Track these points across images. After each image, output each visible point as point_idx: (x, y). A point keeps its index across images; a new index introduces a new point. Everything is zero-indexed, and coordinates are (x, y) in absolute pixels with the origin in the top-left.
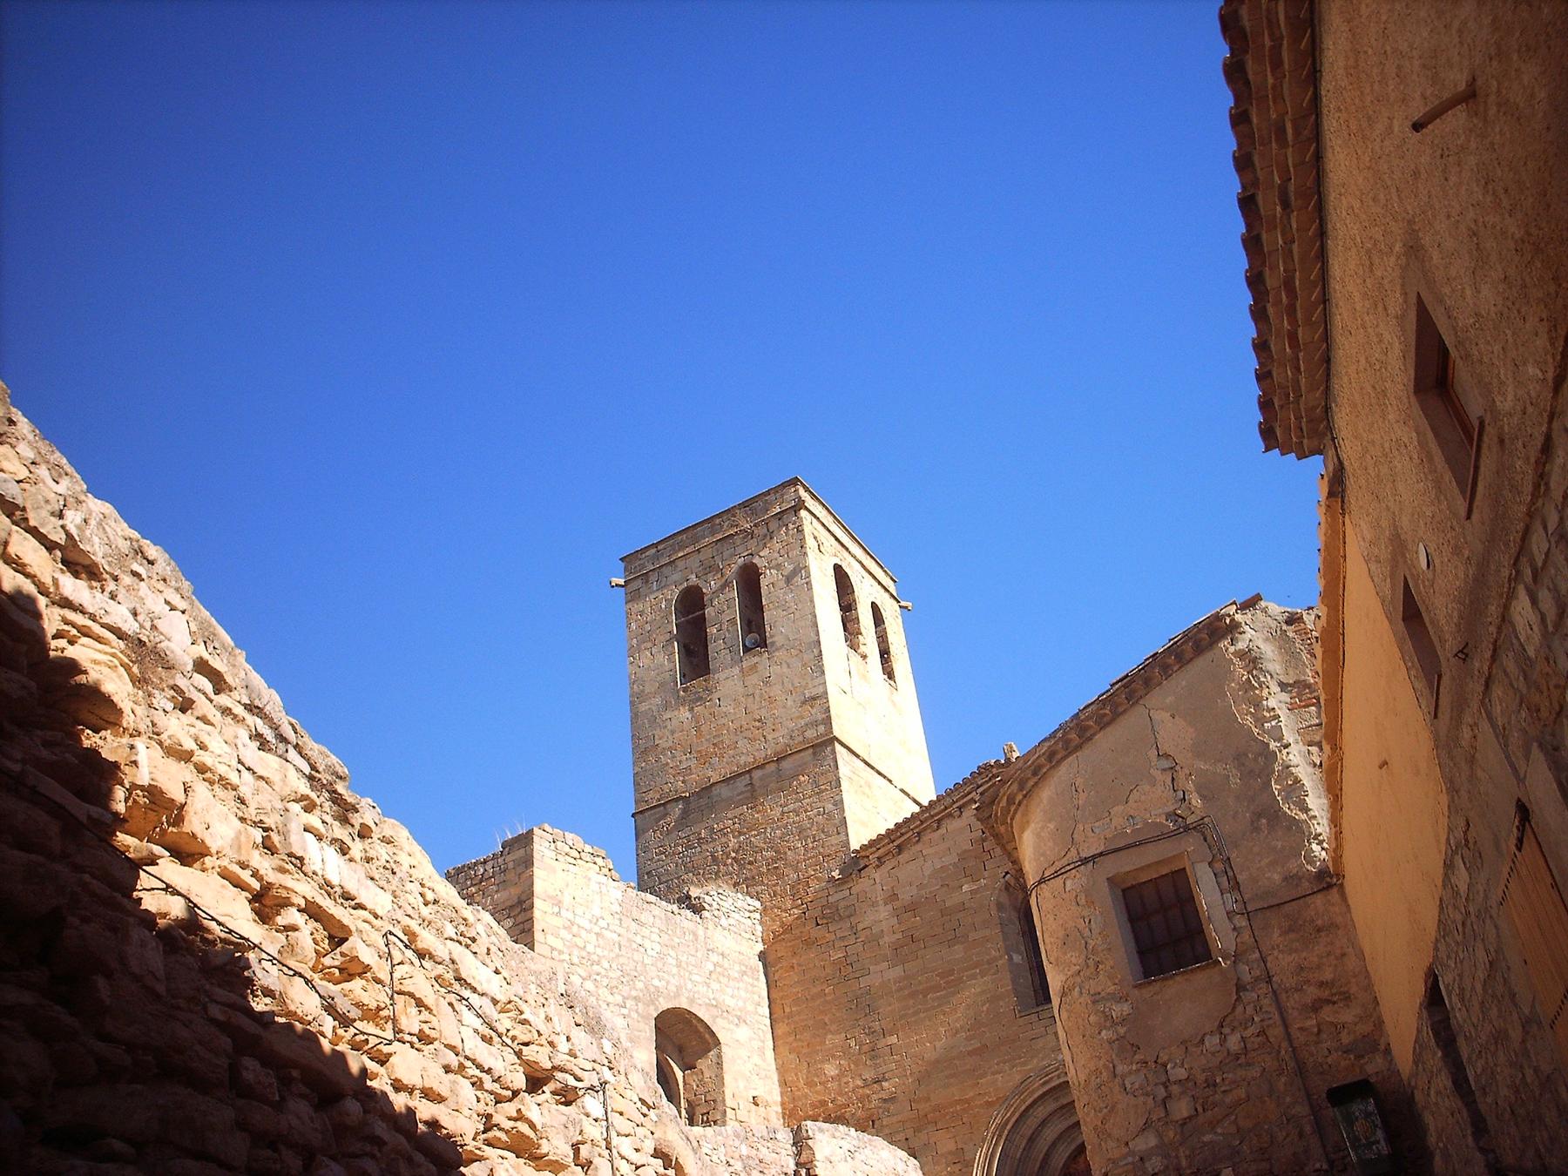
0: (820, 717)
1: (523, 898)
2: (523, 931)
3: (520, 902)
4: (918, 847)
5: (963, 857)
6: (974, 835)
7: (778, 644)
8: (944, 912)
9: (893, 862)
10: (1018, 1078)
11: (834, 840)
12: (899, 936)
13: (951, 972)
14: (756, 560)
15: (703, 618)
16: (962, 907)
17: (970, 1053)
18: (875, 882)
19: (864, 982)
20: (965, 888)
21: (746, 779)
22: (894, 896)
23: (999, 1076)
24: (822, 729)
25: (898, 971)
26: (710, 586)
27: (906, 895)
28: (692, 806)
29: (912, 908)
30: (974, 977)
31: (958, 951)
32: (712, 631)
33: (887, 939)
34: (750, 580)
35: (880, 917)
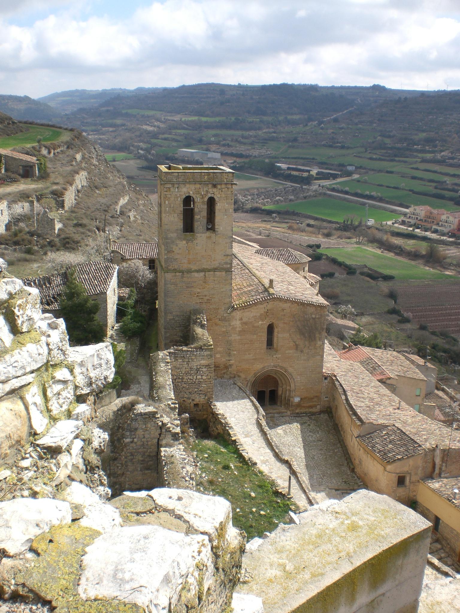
0: (229, 262)
1: (210, 364)
2: (210, 373)
3: (208, 365)
4: (251, 309)
5: (261, 315)
6: (265, 310)
7: (219, 233)
8: (253, 327)
9: (243, 311)
10: (262, 366)
11: (228, 300)
12: (241, 329)
13: (252, 341)
14: (215, 197)
15: (192, 210)
16: (258, 327)
17: (253, 359)
18: (238, 314)
19: (230, 338)
20: (260, 322)
21: (204, 273)
22: (241, 319)
23: (258, 366)
24: (229, 266)
25: (239, 337)
26: (198, 199)
27: (245, 320)
28: (185, 276)
29: (246, 323)
30: (257, 343)
31: (255, 336)
32: (197, 217)
33: (238, 329)
34: (211, 203)
35: (237, 323)
